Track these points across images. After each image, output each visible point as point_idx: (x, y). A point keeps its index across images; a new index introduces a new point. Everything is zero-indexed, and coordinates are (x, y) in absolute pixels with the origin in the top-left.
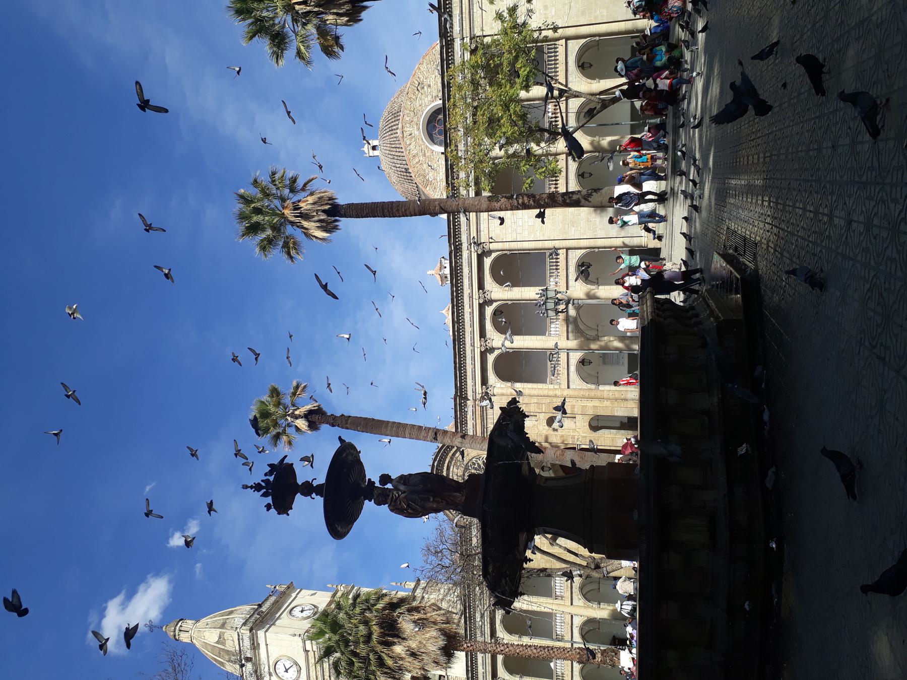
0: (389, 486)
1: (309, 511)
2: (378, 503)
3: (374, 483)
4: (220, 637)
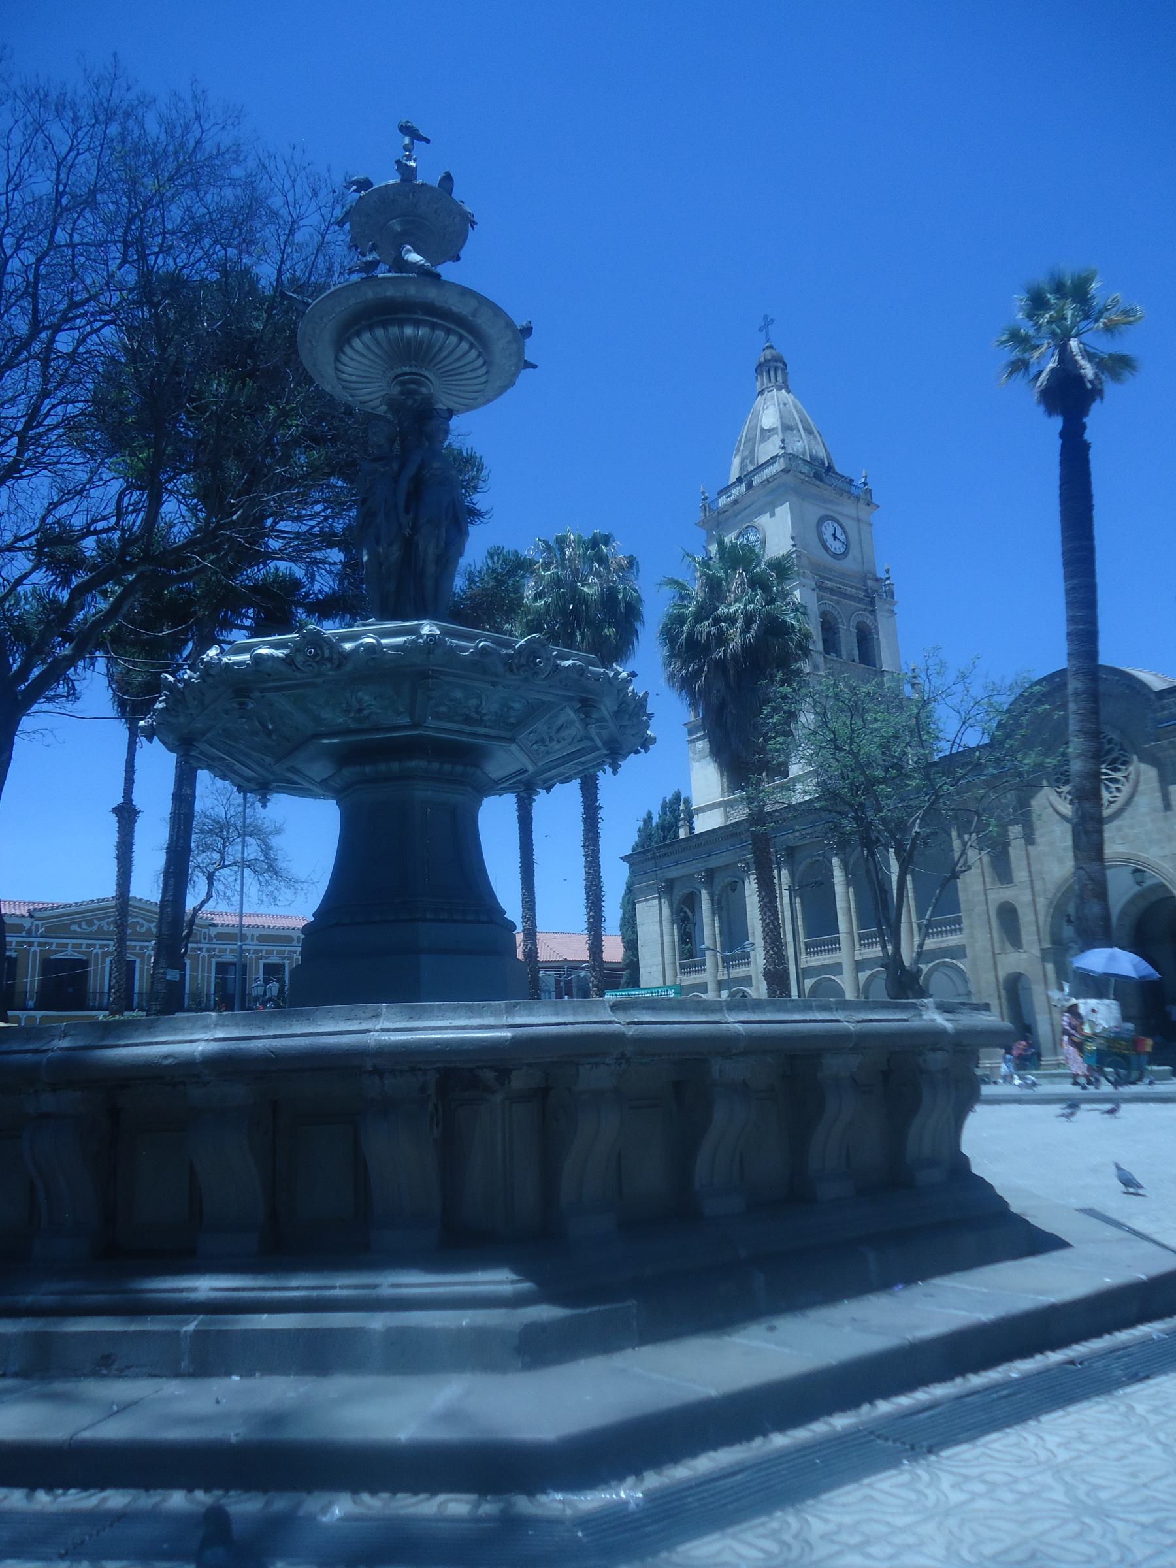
4: (770, 430)
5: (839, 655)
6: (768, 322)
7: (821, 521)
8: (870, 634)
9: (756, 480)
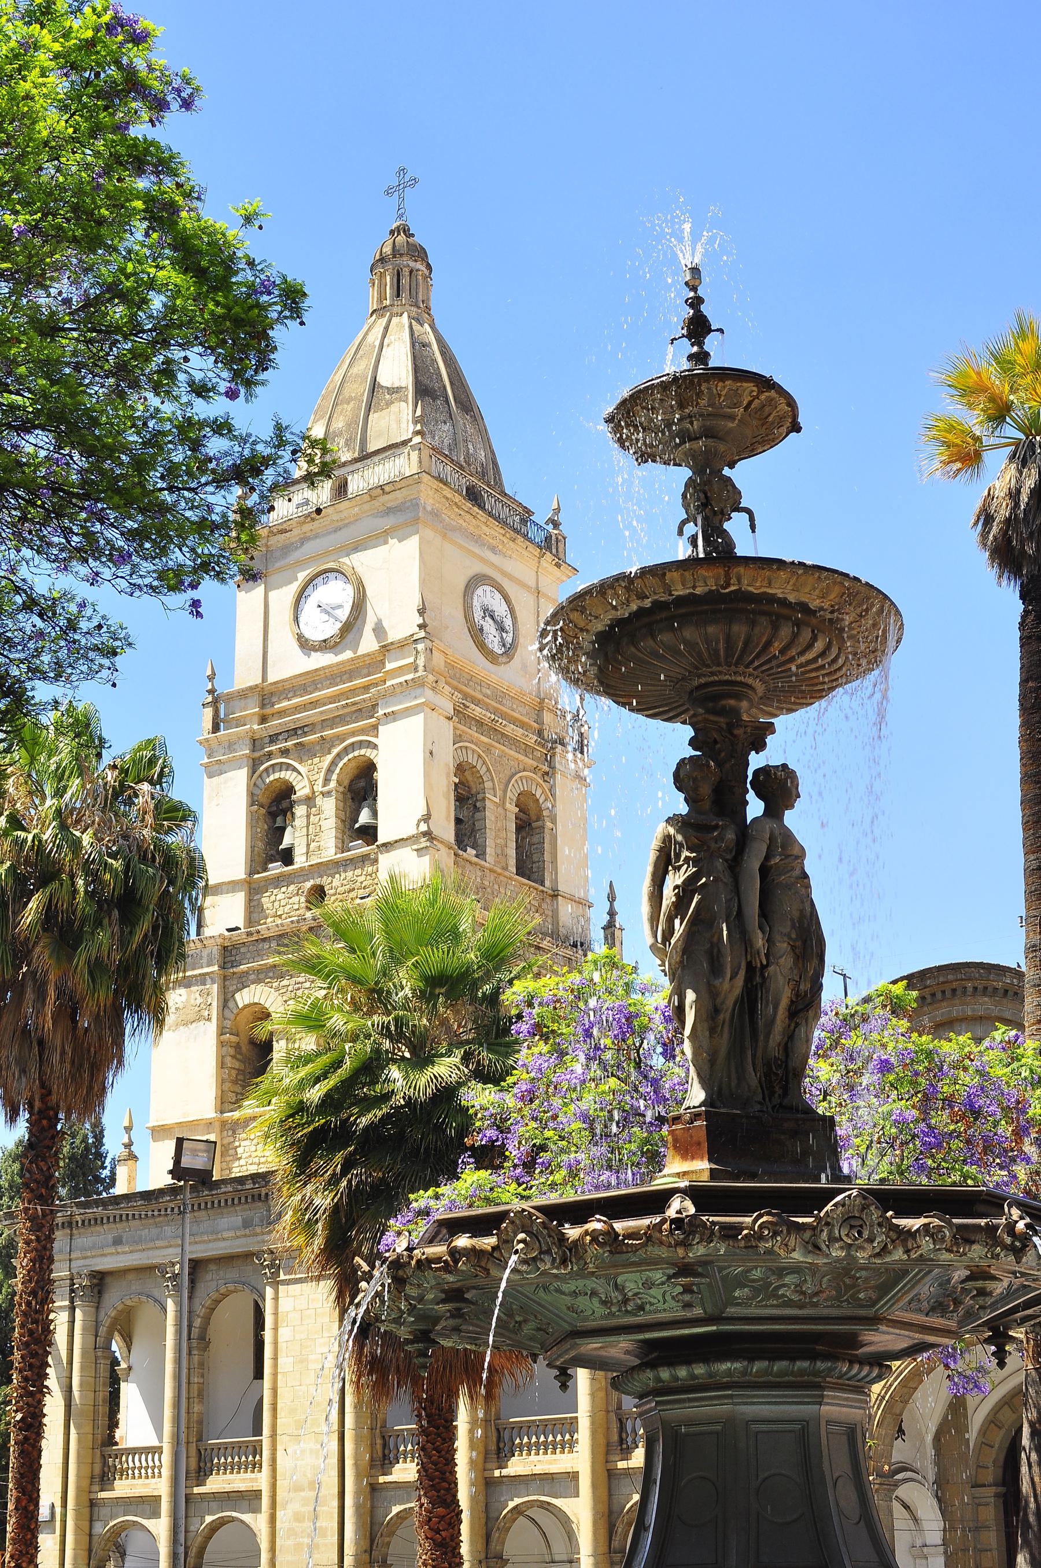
0: (755, 807)
1: (634, 521)
2: (684, 777)
3: (759, 746)
5: (481, 855)
6: (404, 183)
7: (475, 582)
8: (539, 817)
9: (356, 484)
